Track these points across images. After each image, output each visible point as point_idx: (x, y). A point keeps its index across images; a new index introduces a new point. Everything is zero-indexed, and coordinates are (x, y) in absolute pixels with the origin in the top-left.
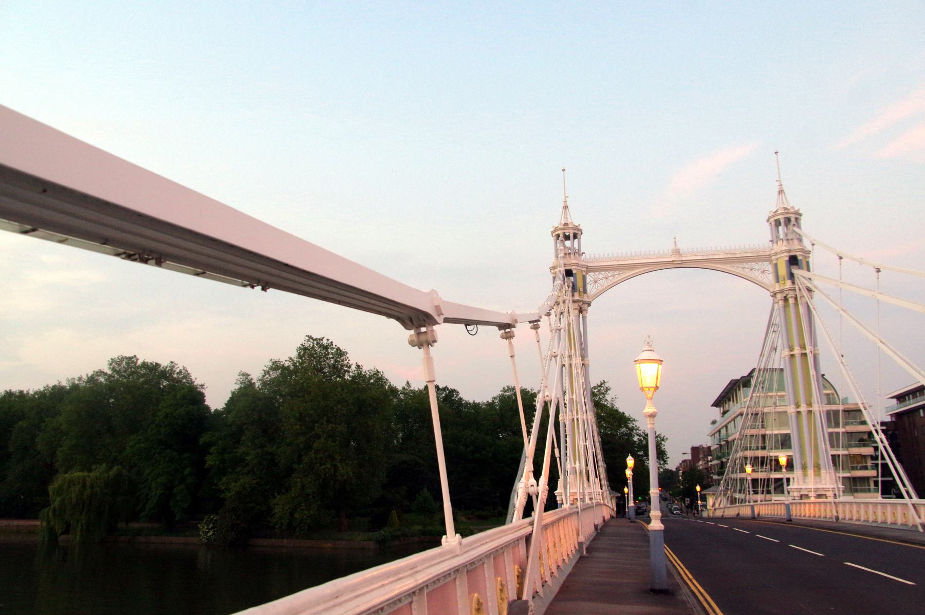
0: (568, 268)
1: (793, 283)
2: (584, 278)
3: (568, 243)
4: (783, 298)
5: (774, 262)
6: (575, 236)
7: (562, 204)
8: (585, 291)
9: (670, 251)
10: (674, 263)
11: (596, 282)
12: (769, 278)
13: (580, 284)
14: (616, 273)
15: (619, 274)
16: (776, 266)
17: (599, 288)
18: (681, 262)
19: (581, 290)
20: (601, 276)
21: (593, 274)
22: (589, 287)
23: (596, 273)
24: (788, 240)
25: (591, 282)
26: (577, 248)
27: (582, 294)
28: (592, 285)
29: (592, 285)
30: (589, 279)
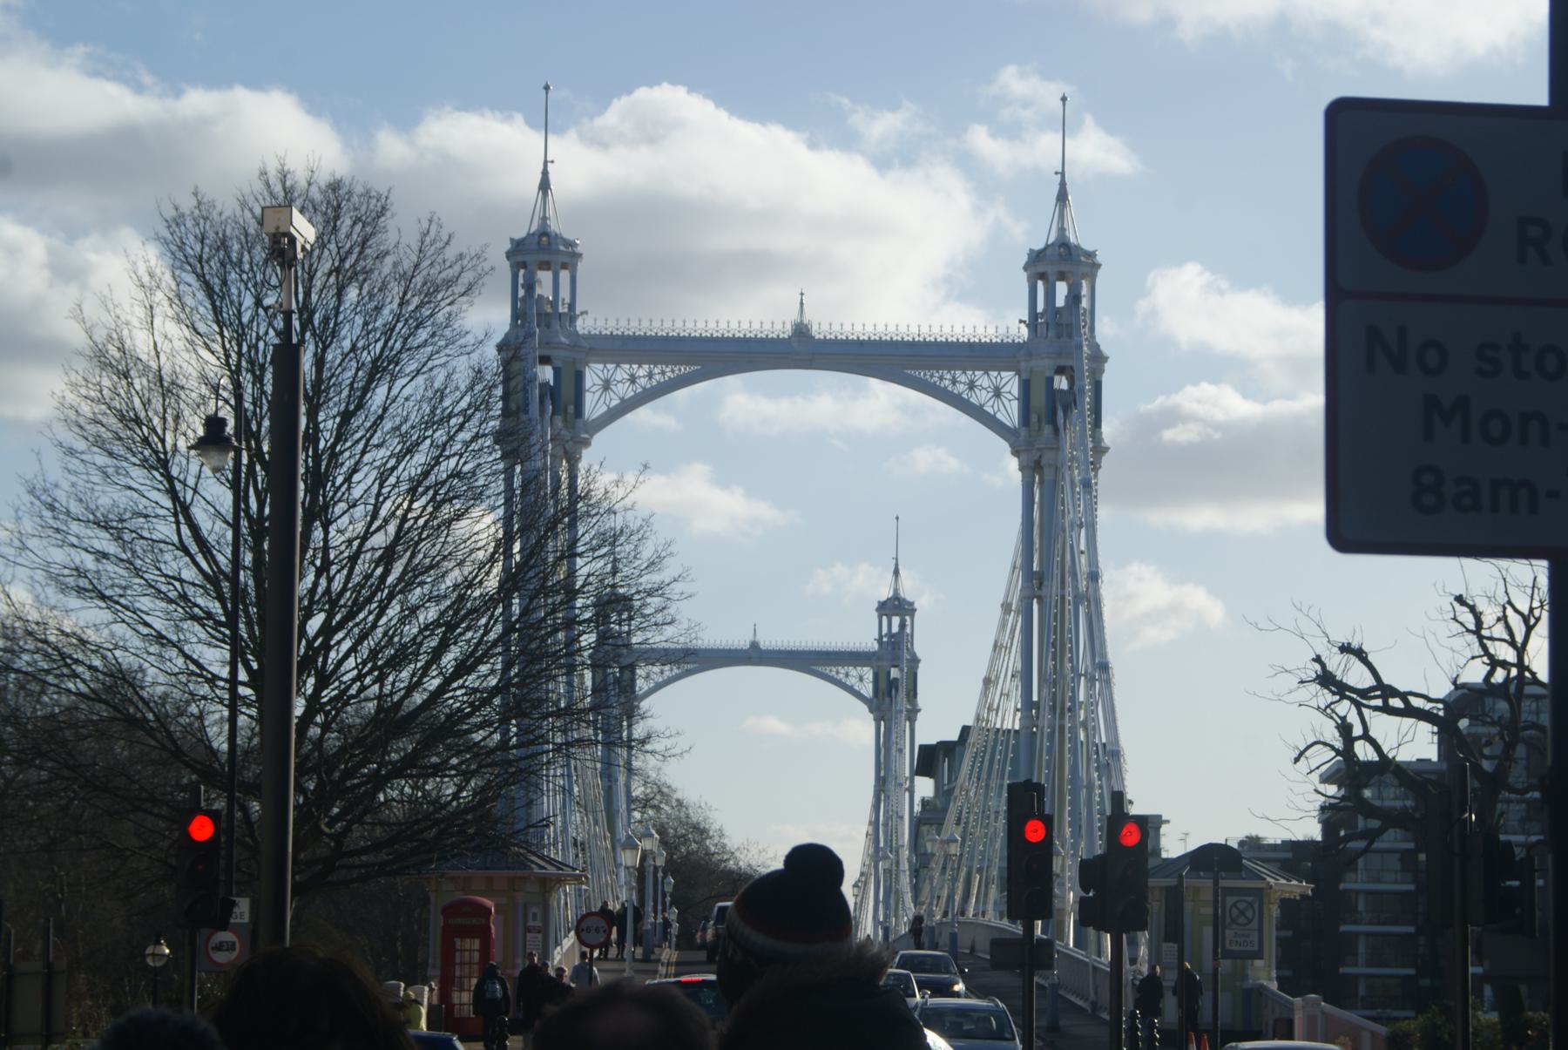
4: (1032, 465)
5: (1025, 376)
7: (539, 176)
9: (789, 327)
12: (1009, 412)
15: (663, 373)
16: (1025, 387)
19: (571, 409)
22: (589, 400)
24: (1058, 325)
25: (593, 390)
26: (567, 300)
30: (593, 375)
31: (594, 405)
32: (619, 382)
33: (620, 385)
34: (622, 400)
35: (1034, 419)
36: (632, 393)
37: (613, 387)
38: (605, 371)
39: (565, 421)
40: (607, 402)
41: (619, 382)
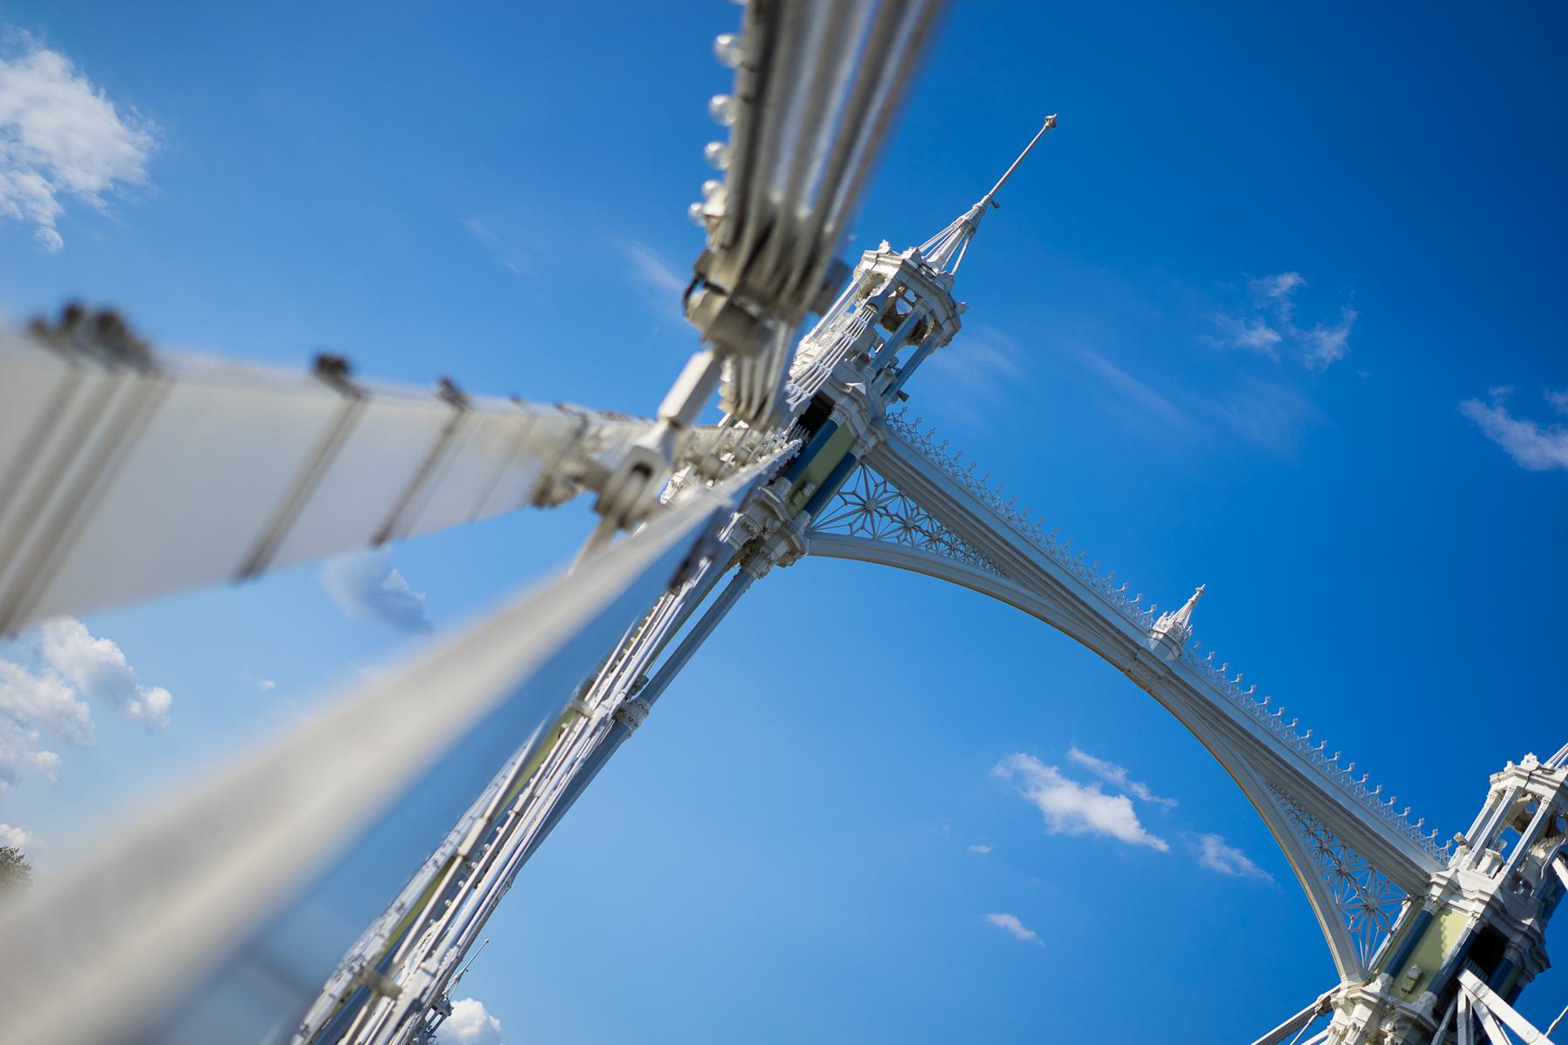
0: (831, 393)
1: (1438, 1014)
2: (846, 464)
3: (885, 334)
6: (917, 333)
8: (813, 505)
10: (1139, 656)
11: (866, 508)
13: (820, 468)
14: (946, 537)
15: (952, 549)
17: (861, 534)
18: (1161, 673)
19: (809, 491)
20: (895, 506)
21: (880, 479)
22: (834, 505)
23: (890, 487)
26: (900, 366)
27: (800, 500)
28: (851, 508)
29: (851, 508)
30: (854, 482)
31: (836, 514)
32: (888, 514)
33: (886, 519)
34: (876, 538)
35: (1412, 971)
36: (895, 541)
37: (876, 515)
38: (881, 489)
39: (792, 498)
40: (855, 527)
41: (888, 514)
